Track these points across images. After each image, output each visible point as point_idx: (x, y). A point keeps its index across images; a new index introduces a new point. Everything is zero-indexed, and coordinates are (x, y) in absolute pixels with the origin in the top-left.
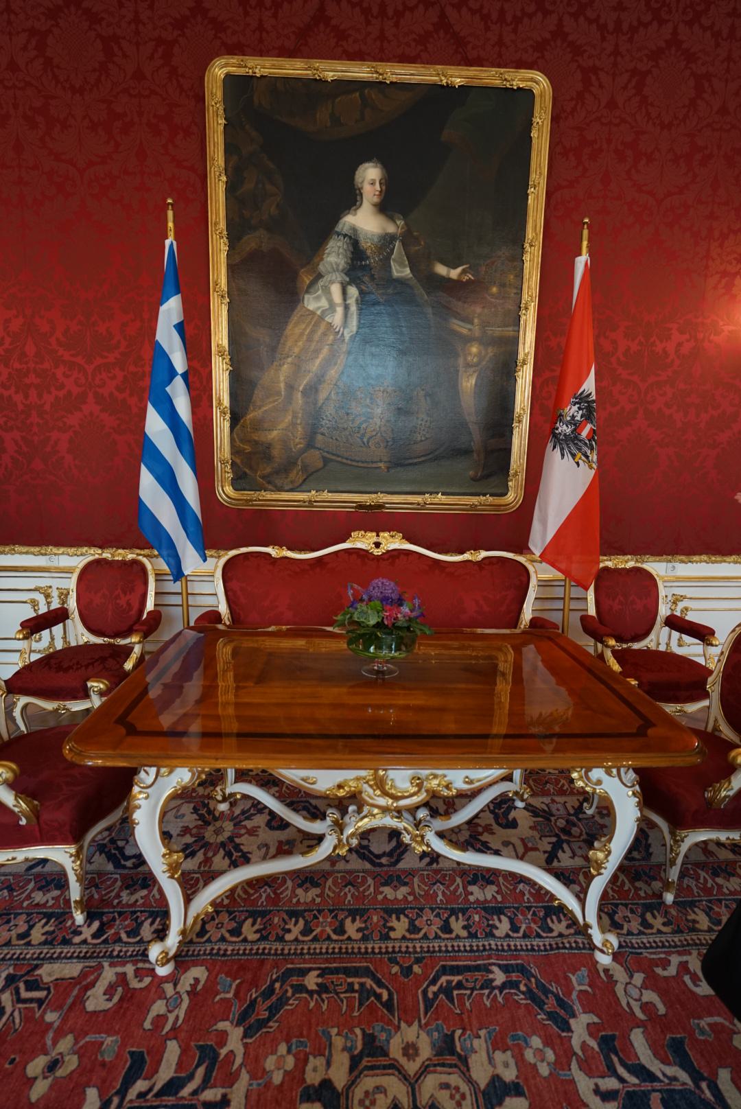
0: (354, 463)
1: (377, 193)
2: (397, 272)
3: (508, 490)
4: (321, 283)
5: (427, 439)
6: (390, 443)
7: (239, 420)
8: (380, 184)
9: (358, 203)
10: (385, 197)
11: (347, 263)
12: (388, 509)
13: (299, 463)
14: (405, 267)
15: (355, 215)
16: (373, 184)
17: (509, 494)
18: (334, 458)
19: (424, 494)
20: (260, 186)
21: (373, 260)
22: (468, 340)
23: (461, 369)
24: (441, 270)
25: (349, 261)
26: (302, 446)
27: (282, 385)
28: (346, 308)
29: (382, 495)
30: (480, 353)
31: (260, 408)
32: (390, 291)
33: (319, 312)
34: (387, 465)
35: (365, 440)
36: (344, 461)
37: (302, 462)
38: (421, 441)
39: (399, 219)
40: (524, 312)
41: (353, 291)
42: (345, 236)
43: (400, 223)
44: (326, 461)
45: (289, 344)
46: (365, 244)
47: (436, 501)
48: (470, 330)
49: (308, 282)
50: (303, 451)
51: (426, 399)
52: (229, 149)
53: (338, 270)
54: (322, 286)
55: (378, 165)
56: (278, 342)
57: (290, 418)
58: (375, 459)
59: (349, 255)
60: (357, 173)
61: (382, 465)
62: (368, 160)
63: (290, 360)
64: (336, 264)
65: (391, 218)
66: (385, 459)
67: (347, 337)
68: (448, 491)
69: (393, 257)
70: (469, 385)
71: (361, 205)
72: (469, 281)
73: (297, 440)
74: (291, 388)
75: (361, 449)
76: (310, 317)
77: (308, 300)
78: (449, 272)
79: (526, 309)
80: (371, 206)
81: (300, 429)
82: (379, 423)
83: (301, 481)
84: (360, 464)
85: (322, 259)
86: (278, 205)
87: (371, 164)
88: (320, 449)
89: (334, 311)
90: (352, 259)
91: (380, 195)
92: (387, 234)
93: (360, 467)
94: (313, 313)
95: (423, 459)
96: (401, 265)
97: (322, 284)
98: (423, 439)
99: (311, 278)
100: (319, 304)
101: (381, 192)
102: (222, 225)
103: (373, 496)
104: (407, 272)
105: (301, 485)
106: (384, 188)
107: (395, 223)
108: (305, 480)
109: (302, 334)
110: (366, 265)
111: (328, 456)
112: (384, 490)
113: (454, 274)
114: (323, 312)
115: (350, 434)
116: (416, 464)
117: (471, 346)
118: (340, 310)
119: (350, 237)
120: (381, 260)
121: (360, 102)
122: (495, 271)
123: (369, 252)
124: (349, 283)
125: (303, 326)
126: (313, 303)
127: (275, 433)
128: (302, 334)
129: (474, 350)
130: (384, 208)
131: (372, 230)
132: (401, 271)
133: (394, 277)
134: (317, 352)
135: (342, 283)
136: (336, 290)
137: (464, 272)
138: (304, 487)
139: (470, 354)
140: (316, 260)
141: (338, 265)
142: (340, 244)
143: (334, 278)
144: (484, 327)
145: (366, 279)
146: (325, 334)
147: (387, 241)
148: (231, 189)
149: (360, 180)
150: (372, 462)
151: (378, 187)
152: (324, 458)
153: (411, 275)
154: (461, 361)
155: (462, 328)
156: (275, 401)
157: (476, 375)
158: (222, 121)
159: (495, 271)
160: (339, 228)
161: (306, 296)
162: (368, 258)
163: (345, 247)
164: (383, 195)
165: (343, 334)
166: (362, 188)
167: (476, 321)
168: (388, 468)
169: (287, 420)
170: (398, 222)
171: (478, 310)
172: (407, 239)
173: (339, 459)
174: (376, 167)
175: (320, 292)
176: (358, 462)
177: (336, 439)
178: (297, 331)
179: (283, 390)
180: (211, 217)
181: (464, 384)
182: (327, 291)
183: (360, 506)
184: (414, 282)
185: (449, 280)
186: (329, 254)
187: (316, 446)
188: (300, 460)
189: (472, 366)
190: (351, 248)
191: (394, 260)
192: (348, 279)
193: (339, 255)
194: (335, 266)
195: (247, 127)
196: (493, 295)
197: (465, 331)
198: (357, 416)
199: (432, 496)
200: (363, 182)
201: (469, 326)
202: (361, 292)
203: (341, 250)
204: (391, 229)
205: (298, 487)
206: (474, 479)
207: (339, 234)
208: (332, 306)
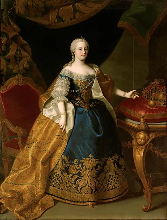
1: (83, 54)
2: (95, 95)
4: (52, 102)
5: (116, 187)
6: (94, 190)
7: (4, 179)
8: (85, 49)
10: (87, 57)
13: (40, 203)
14: (99, 92)
15: (71, 66)
16: (81, 49)
18: (61, 200)
20: (19, 52)
22: (137, 131)
23: (134, 147)
24: (120, 93)
25: (68, 90)
26: (42, 193)
27: (30, 158)
28: (67, 115)
30: (145, 137)
31: (17, 172)
33: (51, 118)
34: (92, 203)
35: (79, 189)
36: (67, 201)
37: (41, 203)
38: (112, 189)
39: (96, 67)
41: (71, 106)
42: (66, 77)
43: (97, 69)
44: (56, 202)
45: (34, 136)
46: (77, 80)
48: (139, 125)
49: (45, 102)
50: (43, 196)
51: (114, 165)
54: (53, 104)
55: (84, 40)
56: (28, 135)
57: (34, 177)
59: (68, 87)
60: (72, 44)
62: (78, 37)
63: (34, 144)
64: (61, 91)
67: (67, 131)
69: (92, 87)
70: (139, 156)
73: (39, 190)
74: (35, 160)
75: (76, 194)
76: (47, 120)
77: (45, 111)
80: (80, 61)
81: (40, 183)
83: (40, 214)
85: (53, 90)
86: (28, 62)
87: (79, 40)
88: (52, 195)
89: (60, 117)
90: (70, 89)
91: (85, 55)
92: (89, 75)
94: (48, 118)
97: (53, 103)
98: (113, 187)
100: (52, 114)
101: (85, 54)
106: (87, 51)
107: (93, 69)
109: (42, 130)
111: (57, 199)
113: (128, 95)
114: (54, 117)
115: (70, 186)
118: (63, 117)
119: (69, 78)
121: (73, 10)
122: (152, 93)
123: (79, 85)
124: (68, 102)
125: (42, 126)
126: (47, 113)
127: (25, 186)
128: (42, 130)
129: (142, 135)
130: (88, 61)
131: (81, 73)
132: (97, 94)
133: (94, 98)
134: (50, 139)
135: (64, 102)
136: (61, 106)
140: (49, 90)
142: (63, 81)
143: (60, 99)
144: (146, 123)
145: (78, 99)
146: (55, 130)
147: (90, 79)
149: (74, 48)
150: (84, 202)
152: (54, 200)
153: (103, 97)
154: (134, 142)
156: (25, 168)
157: (143, 150)
159: (152, 93)
160: (62, 73)
161: (44, 109)
162: (79, 88)
163: (66, 82)
164: (86, 55)
165: (65, 129)
166: (75, 52)
167: (142, 119)
168: (93, 205)
169: (32, 179)
170: (95, 69)
171: (143, 113)
172: (101, 77)
173: (64, 201)
174: (82, 41)
175: (52, 107)
177: (62, 189)
178: (39, 128)
179: (30, 161)
181: (137, 155)
182: (56, 106)
184: (105, 100)
187: (50, 193)
188: (40, 201)
189: (140, 145)
192: (68, 100)
193: (62, 87)
194: (60, 93)
195: (12, 23)
197: (136, 126)
198: (74, 175)
201: (138, 123)
202: (76, 107)
203: (63, 84)
204: (91, 72)
207: (62, 76)
208: (59, 115)
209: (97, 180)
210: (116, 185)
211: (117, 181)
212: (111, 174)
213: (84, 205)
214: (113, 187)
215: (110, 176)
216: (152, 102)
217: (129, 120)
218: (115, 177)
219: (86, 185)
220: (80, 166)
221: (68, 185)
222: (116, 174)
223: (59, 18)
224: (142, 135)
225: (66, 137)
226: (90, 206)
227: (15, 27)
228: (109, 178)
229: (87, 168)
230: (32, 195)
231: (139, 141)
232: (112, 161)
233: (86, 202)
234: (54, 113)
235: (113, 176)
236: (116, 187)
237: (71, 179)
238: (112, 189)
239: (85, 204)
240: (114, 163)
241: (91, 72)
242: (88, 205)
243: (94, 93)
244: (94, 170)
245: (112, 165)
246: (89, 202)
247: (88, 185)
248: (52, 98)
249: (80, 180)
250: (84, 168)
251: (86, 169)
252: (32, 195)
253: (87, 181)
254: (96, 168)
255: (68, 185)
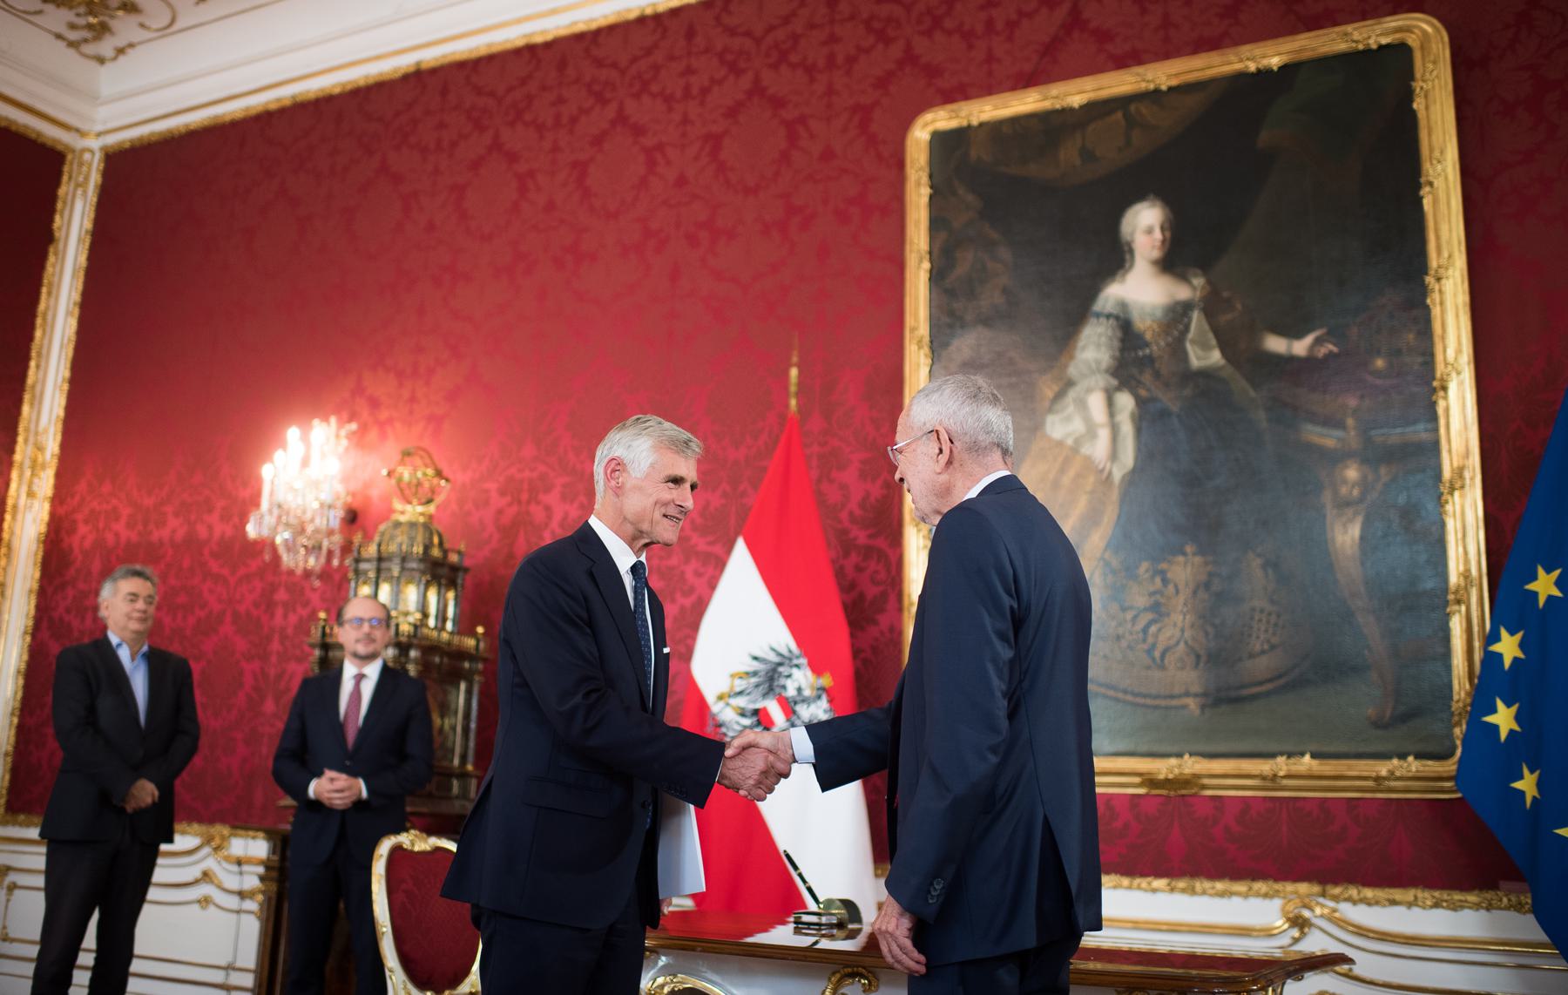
2: (1198, 358)
4: (1072, 394)
5: (1273, 647)
6: (1204, 659)
9: (1127, 265)
11: (1113, 357)
19: (1272, 756)
21: (1157, 347)
22: (1336, 458)
23: (1330, 512)
24: (1276, 344)
25: (1117, 354)
30: (1364, 478)
32: (1188, 392)
33: (1070, 442)
34: (1198, 700)
35: (1157, 654)
38: (1263, 652)
39: (1196, 276)
40: (1441, 393)
41: (1126, 401)
42: (1108, 316)
43: (1198, 281)
46: (1142, 324)
52: (937, 223)
53: (1099, 371)
54: (1074, 401)
58: (1177, 691)
59: (1116, 344)
65: (1183, 277)
66: (1196, 689)
67: (1118, 475)
69: (1191, 335)
71: (1132, 265)
72: (1330, 355)
78: (1290, 347)
79: (1445, 389)
82: (1180, 624)
85: (1072, 357)
90: (1123, 350)
95: (1269, 686)
96: (1205, 347)
99: (1056, 388)
101: (1164, 242)
102: (924, 329)
103: (1173, 761)
104: (1216, 357)
106: (1168, 234)
110: (1145, 356)
113: (1300, 347)
114: (1078, 442)
116: (1254, 697)
117: (1347, 467)
118: (1104, 435)
119: (1117, 318)
120: (1168, 345)
123: (1148, 336)
124: (1118, 389)
129: (1352, 473)
130: (1171, 263)
132: (1205, 356)
136: (1096, 402)
137: (1318, 341)
139: (1345, 482)
141: (1098, 362)
142: (1100, 330)
145: (1147, 378)
147: (1177, 315)
148: (936, 277)
150: (1172, 697)
151: (1158, 235)
154: (1327, 497)
155: (1328, 439)
158: (925, 192)
162: (1147, 345)
166: (1133, 241)
167: (1350, 422)
171: (1352, 402)
172: (1211, 306)
174: (1153, 206)
180: (909, 321)
182: (1082, 405)
183: (1150, 781)
185: (1291, 359)
186: (1084, 348)
189: (1348, 504)
190: (1119, 334)
191: (1193, 342)
192: (1115, 382)
196: (1378, 374)
197: (1330, 443)
200: (1132, 234)
201: (1339, 433)
202: (1140, 402)
203: (1103, 339)
204: (1183, 293)
206: (1378, 724)
207: (1098, 315)
208: (1091, 433)
209: (1214, 625)
210: (1275, 640)
211: (1276, 625)
212: (1257, 603)
214: (1266, 647)
215: (1253, 609)
216: (1380, 363)
217: (1309, 428)
218: (1270, 614)
219: (1178, 643)
220: (1158, 580)
221: (1124, 644)
222: (1272, 602)
223: (1087, 155)
224: (1352, 473)
225: (1115, 495)
227: (970, 198)
228: (1252, 618)
229: (1181, 587)
230: (432, 622)
231: (1344, 490)
232: (1259, 561)
233: (1180, 696)
234: (1077, 426)
235: (1262, 611)
236: (1273, 647)
237: (1133, 625)
238: (1263, 652)
239: (1175, 702)
240: (1264, 567)
241: (1183, 293)
243: (1195, 352)
244: (1202, 594)
245: (1259, 573)
247: (1186, 643)
248: (1070, 384)
249: (1158, 625)
250: (1171, 588)
251: (1177, 592)
252: (432, 622)
253: (1182, 631)
254: (1207, 586)
255: (1124, 644)
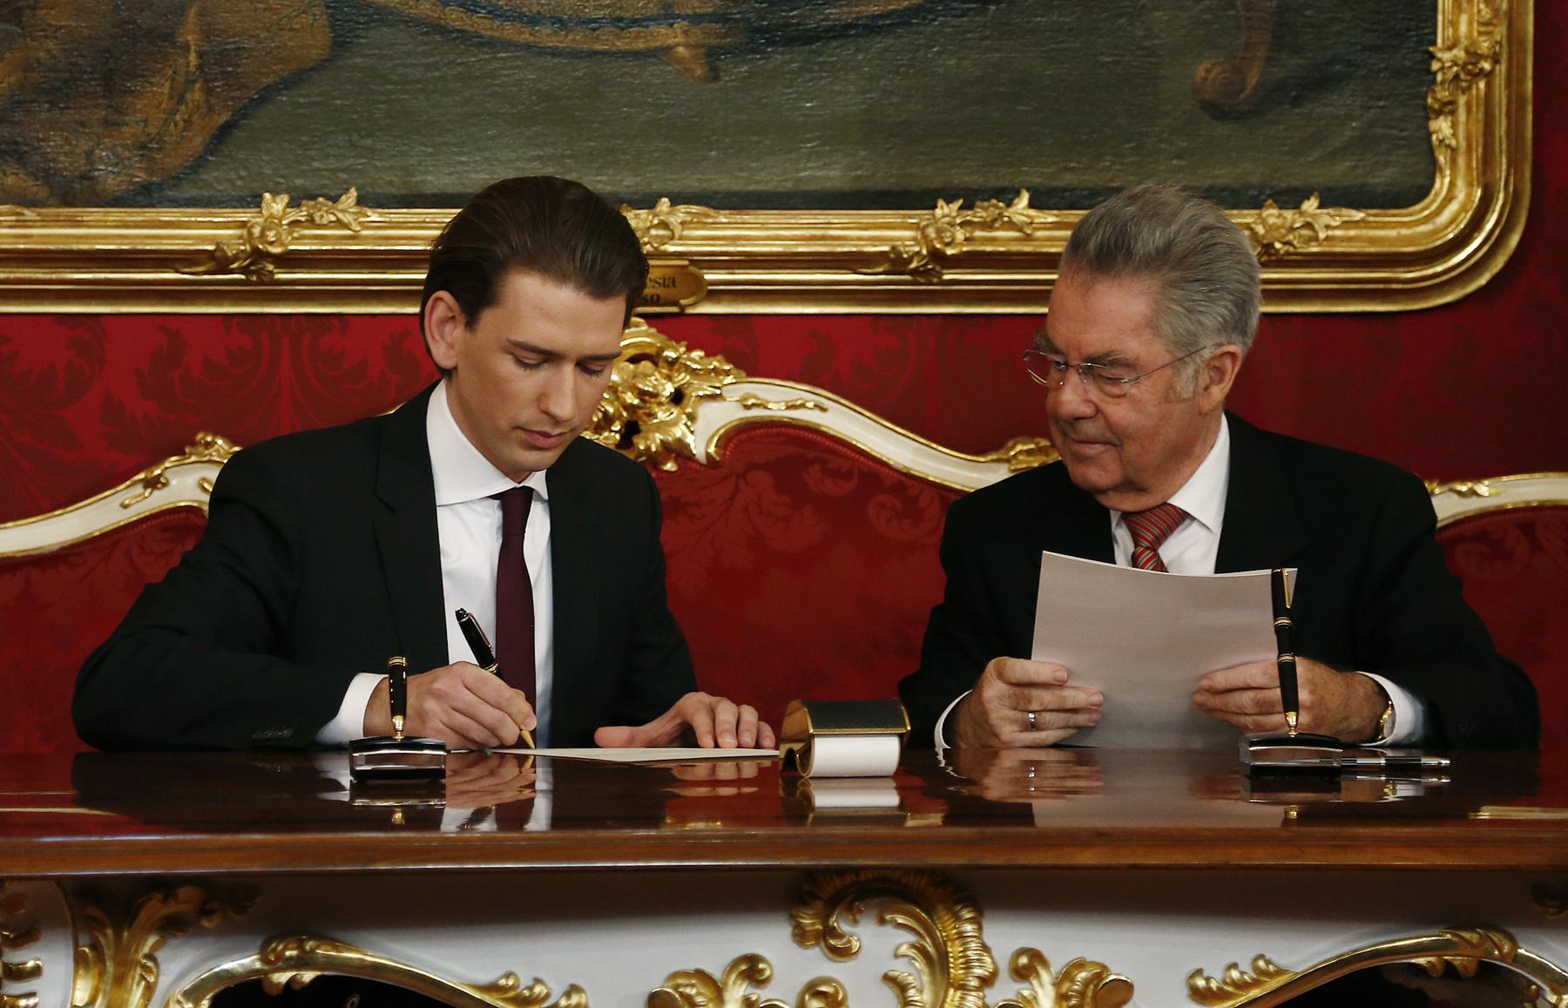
0: (509, 31)
3: (1433, 168)
12: (714, 295)
17: (1441, 184)
19: (923, 199)
29: (682, 212)
47: (1002, 240)
61: (673, 36)
68: (1068, 179)
83: (198, 142)
84: (546, 36)
93: (555, 53)
105: (198, 164)
108: (223, 134)
112: (691, 181)
138: (216, 177)
168: (712, 55)
176: (534, 21)
199: (979, 214)
205: (176, 180)
213: (626, 54)
226: (680, 61)
242: (668, 49)
246: (679, 25)
